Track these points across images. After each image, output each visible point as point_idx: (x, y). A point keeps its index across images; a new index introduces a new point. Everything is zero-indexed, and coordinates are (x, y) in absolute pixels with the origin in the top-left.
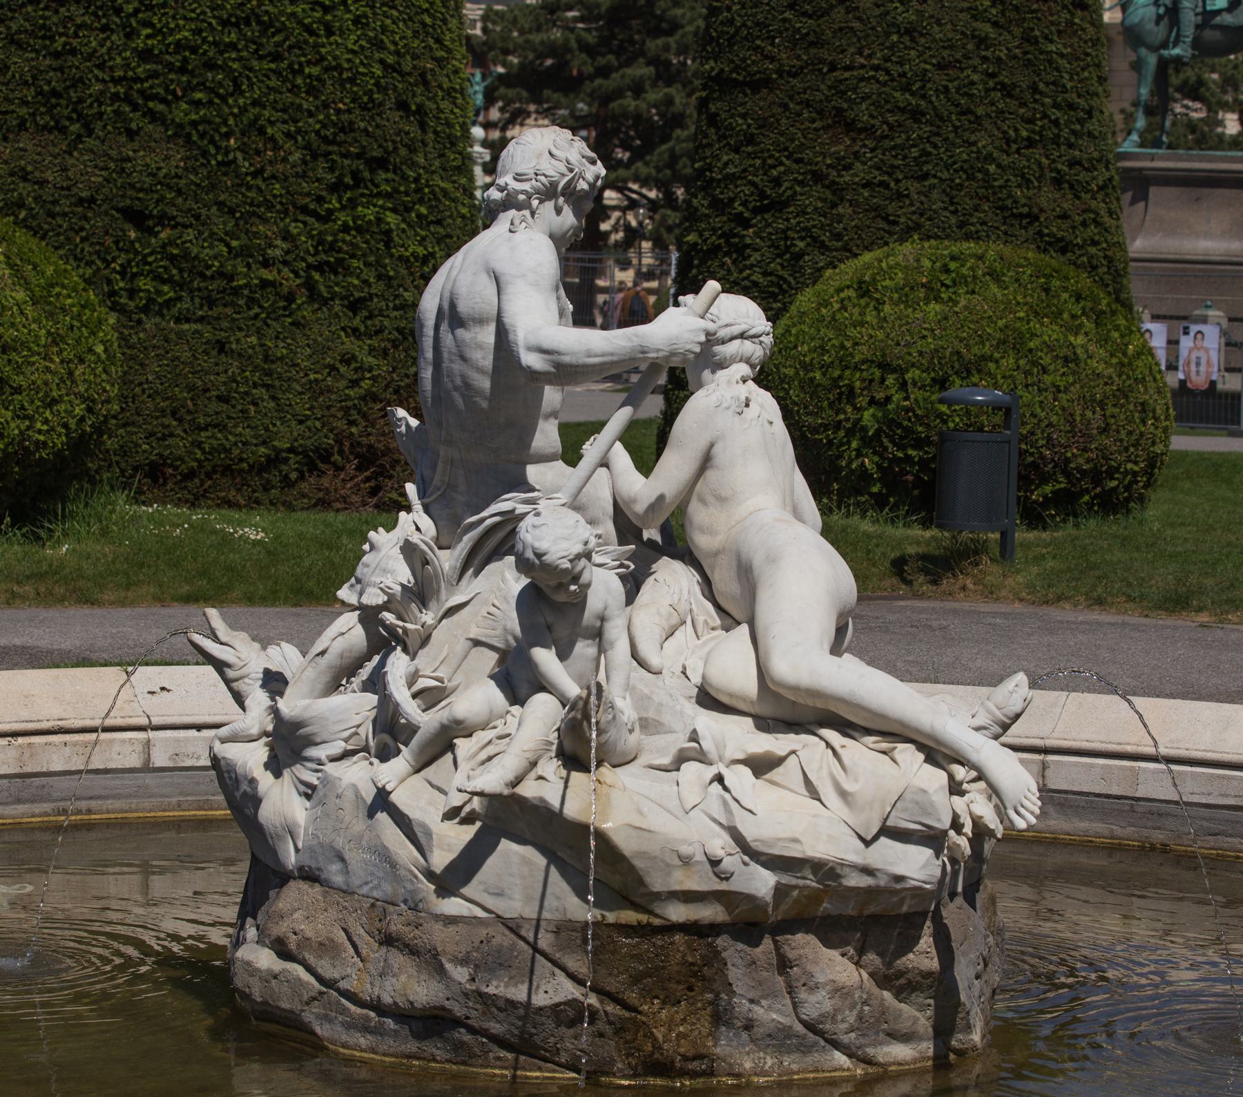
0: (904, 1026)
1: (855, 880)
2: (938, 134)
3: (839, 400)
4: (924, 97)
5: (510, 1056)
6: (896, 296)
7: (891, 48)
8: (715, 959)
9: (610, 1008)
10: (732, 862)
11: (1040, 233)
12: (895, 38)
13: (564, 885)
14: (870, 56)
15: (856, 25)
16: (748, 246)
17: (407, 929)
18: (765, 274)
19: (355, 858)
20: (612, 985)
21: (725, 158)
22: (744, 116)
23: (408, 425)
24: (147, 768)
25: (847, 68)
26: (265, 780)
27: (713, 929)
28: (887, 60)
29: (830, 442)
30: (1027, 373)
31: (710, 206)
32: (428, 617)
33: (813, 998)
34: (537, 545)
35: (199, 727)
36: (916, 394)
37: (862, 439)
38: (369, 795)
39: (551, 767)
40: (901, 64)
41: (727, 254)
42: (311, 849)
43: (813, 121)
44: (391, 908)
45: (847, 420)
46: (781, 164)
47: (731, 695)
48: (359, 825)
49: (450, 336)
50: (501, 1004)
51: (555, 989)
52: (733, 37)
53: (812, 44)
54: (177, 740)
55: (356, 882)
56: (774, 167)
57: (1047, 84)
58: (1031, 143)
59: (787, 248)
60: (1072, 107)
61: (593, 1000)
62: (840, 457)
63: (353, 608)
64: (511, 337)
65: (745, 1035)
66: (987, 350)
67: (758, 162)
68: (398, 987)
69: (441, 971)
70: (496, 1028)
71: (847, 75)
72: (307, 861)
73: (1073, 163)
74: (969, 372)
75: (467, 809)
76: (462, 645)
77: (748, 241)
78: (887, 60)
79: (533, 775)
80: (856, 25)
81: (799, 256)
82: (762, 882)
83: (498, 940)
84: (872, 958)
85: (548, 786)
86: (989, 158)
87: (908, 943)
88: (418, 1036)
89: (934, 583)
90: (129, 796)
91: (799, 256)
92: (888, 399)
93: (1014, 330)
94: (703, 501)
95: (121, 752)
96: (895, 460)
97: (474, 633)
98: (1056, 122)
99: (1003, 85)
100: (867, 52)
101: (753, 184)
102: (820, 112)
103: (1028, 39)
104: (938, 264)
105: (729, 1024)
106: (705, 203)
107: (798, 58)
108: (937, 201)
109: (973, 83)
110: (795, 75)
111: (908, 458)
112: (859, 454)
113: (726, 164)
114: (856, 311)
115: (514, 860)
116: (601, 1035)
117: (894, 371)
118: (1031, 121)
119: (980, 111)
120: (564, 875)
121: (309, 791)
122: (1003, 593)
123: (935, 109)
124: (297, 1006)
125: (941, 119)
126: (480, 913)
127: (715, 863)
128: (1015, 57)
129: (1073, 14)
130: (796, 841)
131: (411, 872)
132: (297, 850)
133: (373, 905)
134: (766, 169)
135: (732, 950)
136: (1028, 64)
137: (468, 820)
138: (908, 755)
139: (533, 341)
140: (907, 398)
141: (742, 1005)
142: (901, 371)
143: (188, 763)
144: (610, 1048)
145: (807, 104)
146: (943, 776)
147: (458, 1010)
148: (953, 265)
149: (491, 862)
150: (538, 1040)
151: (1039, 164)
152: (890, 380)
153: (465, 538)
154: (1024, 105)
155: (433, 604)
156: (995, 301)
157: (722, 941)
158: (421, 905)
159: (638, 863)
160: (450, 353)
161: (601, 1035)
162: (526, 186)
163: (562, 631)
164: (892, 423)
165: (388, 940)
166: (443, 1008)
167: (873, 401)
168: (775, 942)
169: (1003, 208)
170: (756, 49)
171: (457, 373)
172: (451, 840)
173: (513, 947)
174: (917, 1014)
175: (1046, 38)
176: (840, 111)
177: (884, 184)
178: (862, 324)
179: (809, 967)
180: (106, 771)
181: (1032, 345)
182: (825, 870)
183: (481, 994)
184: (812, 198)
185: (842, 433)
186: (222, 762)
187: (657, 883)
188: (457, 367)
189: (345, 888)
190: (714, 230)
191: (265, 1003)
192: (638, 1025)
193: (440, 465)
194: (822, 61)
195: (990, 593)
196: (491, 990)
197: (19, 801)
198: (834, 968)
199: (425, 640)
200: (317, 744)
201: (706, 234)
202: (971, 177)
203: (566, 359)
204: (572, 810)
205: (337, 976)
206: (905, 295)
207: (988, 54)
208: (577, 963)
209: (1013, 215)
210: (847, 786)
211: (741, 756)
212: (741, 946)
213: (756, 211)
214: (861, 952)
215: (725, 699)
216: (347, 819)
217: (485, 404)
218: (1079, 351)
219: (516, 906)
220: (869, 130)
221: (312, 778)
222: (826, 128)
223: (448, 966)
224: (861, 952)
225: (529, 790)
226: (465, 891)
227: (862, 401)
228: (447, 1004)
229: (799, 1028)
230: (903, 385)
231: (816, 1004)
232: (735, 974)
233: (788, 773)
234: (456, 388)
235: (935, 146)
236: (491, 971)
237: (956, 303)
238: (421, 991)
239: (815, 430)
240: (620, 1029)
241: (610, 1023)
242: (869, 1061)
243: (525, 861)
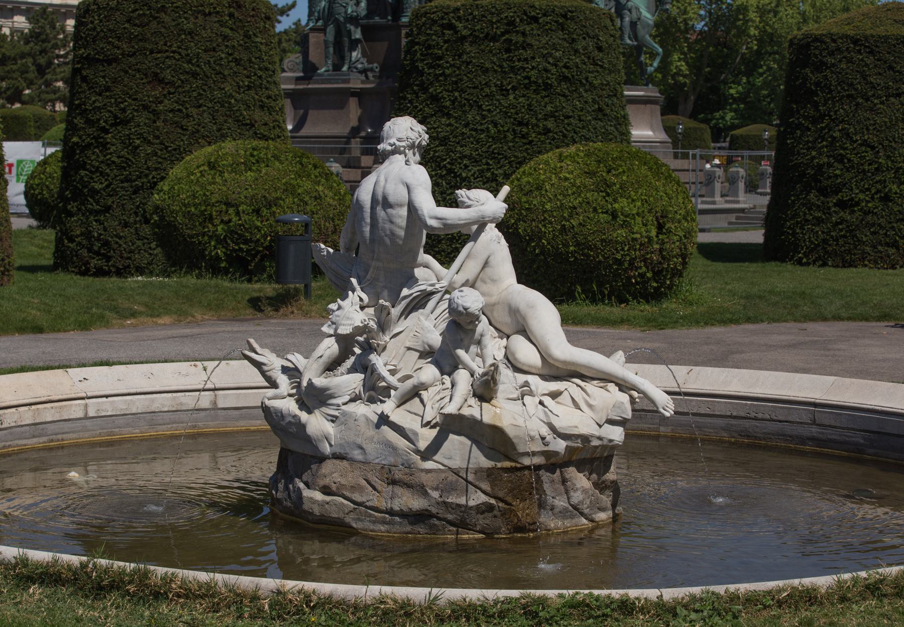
0: (603, 505)
1: (595, 443)
2: (206, 85)
3: (205, 221)
4: (198, 66)
5: (455, 529)
6: (230, 169)
7: (181, 42)
8: (539, 480)
9: (500, 504)
10: (550, 437)
11: (256, 133)
12: (183, 36)
13: (479, 452)
14: (171, 46)
15: (163, 30)
16: (108, 143)
18: (119, 157)
19: (369, 447)
20: (501, 494)
21: (93, 99)
22: (104, 77)
23: (328, 251)
24: (86, 418)
25: (159, 52)
26: (304, 416)
27: (538, 468)
28: (179, 47)
29: (200, 243)
30: (298, 205)
31: (86, 123)
32: (387, 338)
33: (576, 495)
34: (465, 304)
35: (107, 396)
36: (245, 217)
37: (216, 240)
38: (375, 419)
39: (473, 401)
40: (187, 50)
41: (95, 147)
42: (341, 445)
43: (142, 79)
45: (209, 231)
46: (126, 101)
47: (529, 366)
48: (372, 432)
50: (454, 506)
51: (477, 498)
52: (95, 37)
53: (141, 40)
54: (99, 403)
55: (370, 458)
56: (122, 103)
57: (256, 58)
58: (249, 88)
59: (130, 144)
60: (267, 69)
61: (493, 501)
62: (205, 249)
63: (331, 336)
64: (420, 212)
65: (550, 512)
66: (279, 194)
67: (113, 100)
68: (402, 502)
69: (425, 494)
70: (450, 517)
71: (159, 55)
72: (338, 450)
73: (269, 97)
74: (270, 206)
75: (434, 422)
76: (403, 349)
77: (109, 140)
78: (179, 47)
79: (466, 405)
80: (163, 30)
81: (137, 148)
82: (560, 445)
83: (450, 478)
84: (594, 476)
85: (473, 409)
86: (231, 96)
87: (607, 469)
88: (411, 524)
89: (277, 310)
90: (79, 431)
91: (137, 148)
92: (230, 221)
93: (290, 184)
94: (484, 282)
95: (75, 410)
96: (234, 250)
97: (408, 344)
98: (260, 77)
99: (236, 60)
100: (169, 44)
101: (110, 111)
102: (146, 75)
103: (247, 36)
104: (248, 153)
105: (544, 508)
106: (82, 121)
107: (133, 47)
108: (207, 118)
109: (222, 59)
110: (131, 56)
111: (241, 249)
112: (215, 248)
113: (94, 102)
114: (210, 177)
115: (456, 444)
116: (495, 517)
117: (233, 206)
118: (248, 77)
119: (226, 73)
120: (479, 448)
121: (333, 419)
122: (313, 314)
123: (204, 72)
124: (341, 515)
125: (207, 77)
126: (442, 467)
127: (543, 438)
128: (241, 45)
129: (265, 23)
130: (576, 427)
132: (331, 445)
134: (117, 104)
135: (545, 476)
136: (247, 48)
137: (433, 427)
138: (612, 387)
139: (432, 214)
140: (240, 220)
141: (550, 500)
142: (236, 206)
143: (103, 414)
144: (499, 522)
145: (139, 71)
146: (627, 396)
147: (434, 510)
148: (255, 153)
149: (446, 444)
150: (468, 521)
151: (254, 98)
152: (231, 211)
153: (403, 302)
154: (245, 69)
155: (387, 332)
156: (279, 170)
157: (542, 472)
159: (514, 440)
161: (495, 517)
162: (403, 144)
163: (466, 342)
164: (232, 232)
165: (393, 482)
166: (427, 510)
167: (222, 221)
168: (561, 472)
169: (238, 121)
170: (109, 43)
172: (427, 436)
173: (457, 481)
174: (606, 499)
175: (254, 35)
176: (156, 74)
177: (179, 110)
178: (214, 183)
179: (574, 481)
180: (69, 420)
181: (299, 191)
182: (585, 439)
183: (444, 502)
184: (143, 118)
185: (206, 238)
187: (521, 449)
188: (388, 226)
190: (89, 135)
191: (322, 515)
192: (511, 511)
193: (371, 270)
194: (146, 49)
195: (306, 314)
196: (449, 500)
197: (34, 437)
198: (581, 481)
199: (385, 348)
201: (84, 137)
202: (223, 106)
203: (449, 222)
204: (487, 419)
205: (364, 500)
206: (234, 168)
207: (228, 44)
208: (486, 486)
209: (243, 124)
210: (592, 402)
211: (547, 392)
212: (548, 474)
213: (112, 125)
214: (590, 474)
215: (525, 368)
216: (363, 430)
217: (401, 242)
218: (321, 193)
219: (457, 463)
220: (172, 83)
221: (336, 413)
222: (149, 83)
223: (429, 491)
224: (590, 474)
225: (466, 412)
226: (435, 458)
227: (217, 222)
228: (429, 508)
229: (570, 508)
230: (238, 213)
231: (576, 497)
232: (546, 486)
233: (565, 398)
234: (386, 235)
235: (204, 91)
236: (449, 492)
237: (261, 172)
238: (416, 503)
239: (192, 237)
240: (503, 513)
241: (500, 511)
242: (592, 521)
243: (461, 443)
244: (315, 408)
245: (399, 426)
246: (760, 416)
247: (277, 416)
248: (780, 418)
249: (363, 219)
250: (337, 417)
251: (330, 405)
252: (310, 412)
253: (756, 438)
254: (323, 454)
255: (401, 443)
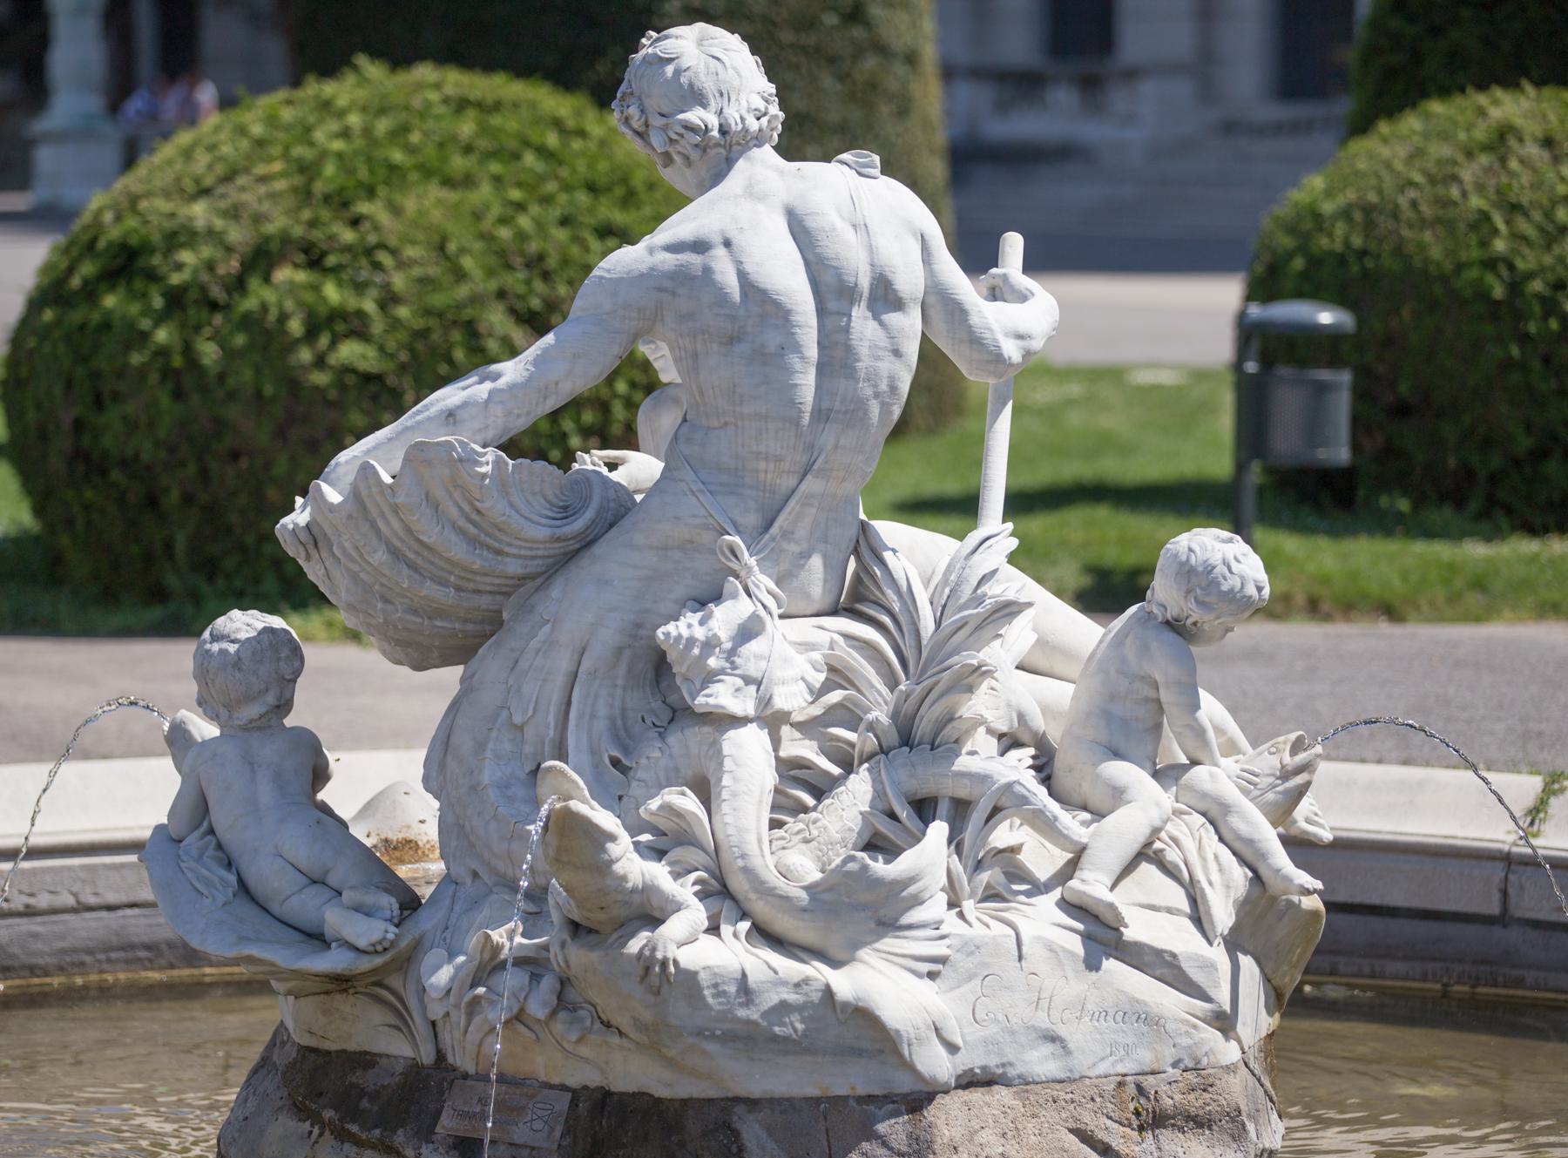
17: (1192, 1097)
19: (1077, 1034)
38: (1075, 944)
44: (1150, 1078)
49: (872, 325)
64: (974, 320)
121: (935, 967)
131: (1186, 1022)
132: (952, 1048)
133: (1121, 1084)
158: (1205, 1061)
160: (874, 346)
171: (885, 374)
186: (702, 976)
189: (1063, 1076)
200: (922, 903)
221: (939, 949)
244: (856, 945)
245: (1159, 953)
246: (43, 901)
247: (720, 994)
248: (112, 898)
249: (797, 348)
250: (942, 960)
251: (910, 927)
252: (835, 964)
253: (32, 970)
254: (934, 1080)
255: (1169, 1001)
